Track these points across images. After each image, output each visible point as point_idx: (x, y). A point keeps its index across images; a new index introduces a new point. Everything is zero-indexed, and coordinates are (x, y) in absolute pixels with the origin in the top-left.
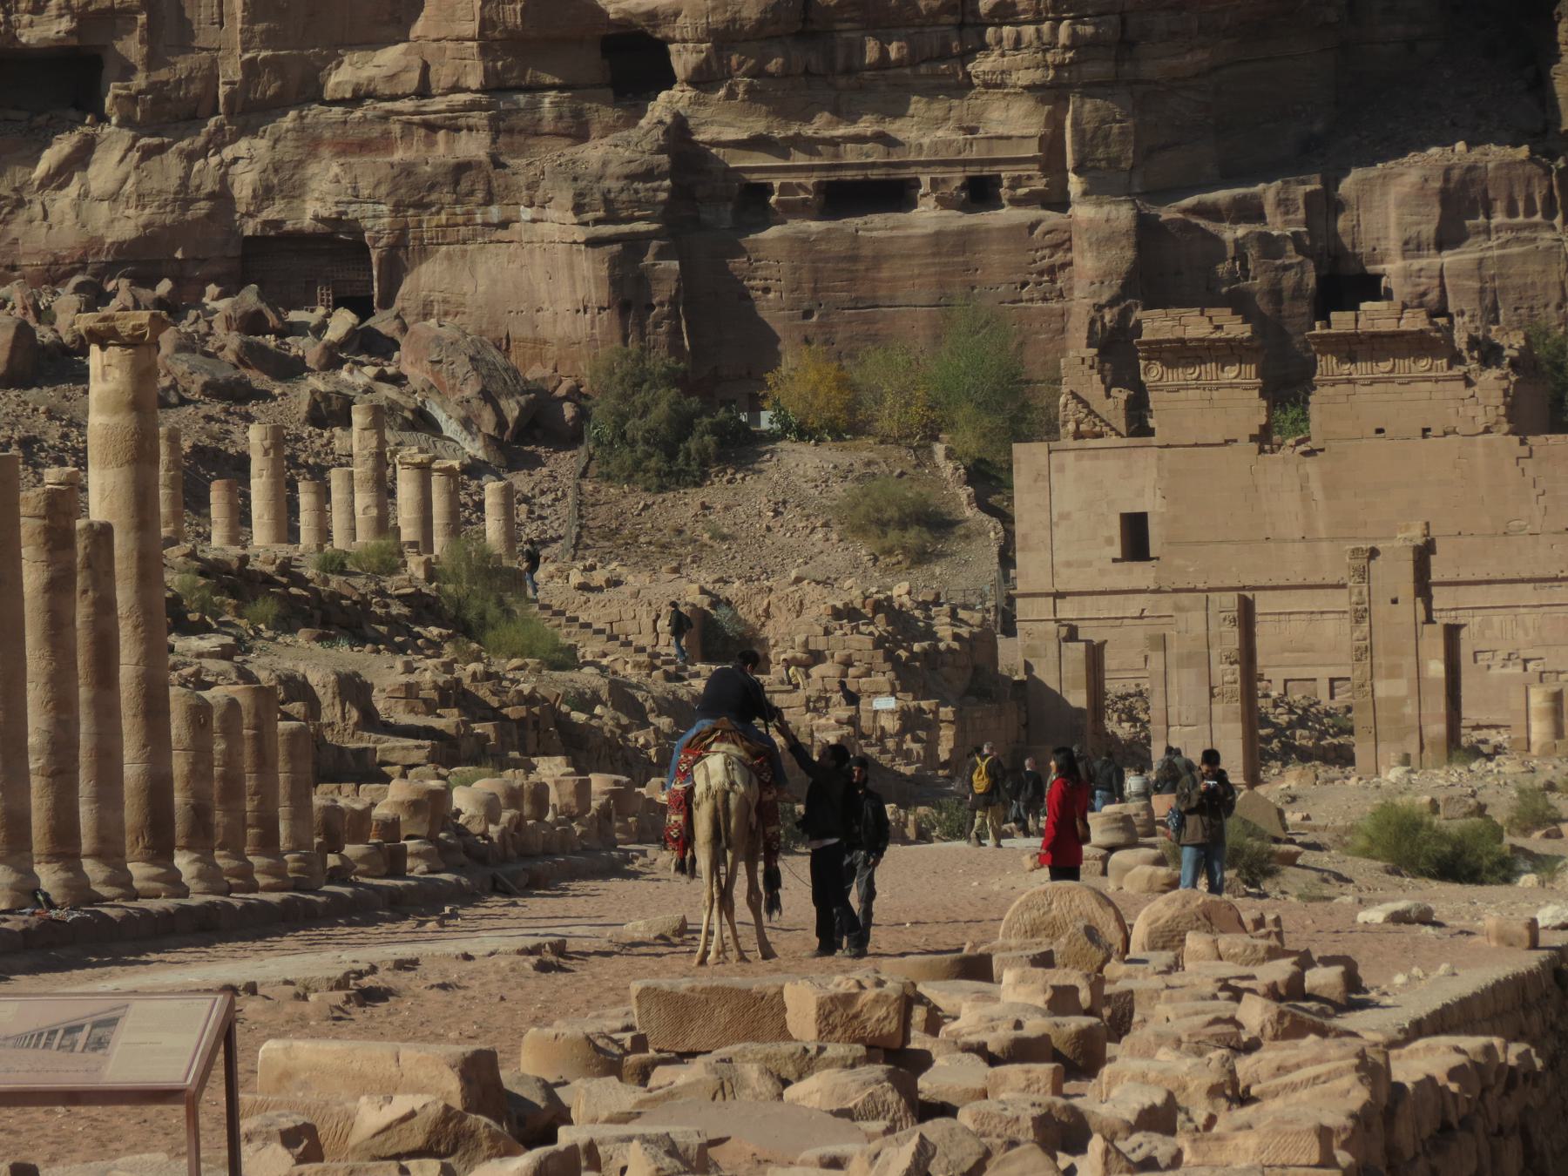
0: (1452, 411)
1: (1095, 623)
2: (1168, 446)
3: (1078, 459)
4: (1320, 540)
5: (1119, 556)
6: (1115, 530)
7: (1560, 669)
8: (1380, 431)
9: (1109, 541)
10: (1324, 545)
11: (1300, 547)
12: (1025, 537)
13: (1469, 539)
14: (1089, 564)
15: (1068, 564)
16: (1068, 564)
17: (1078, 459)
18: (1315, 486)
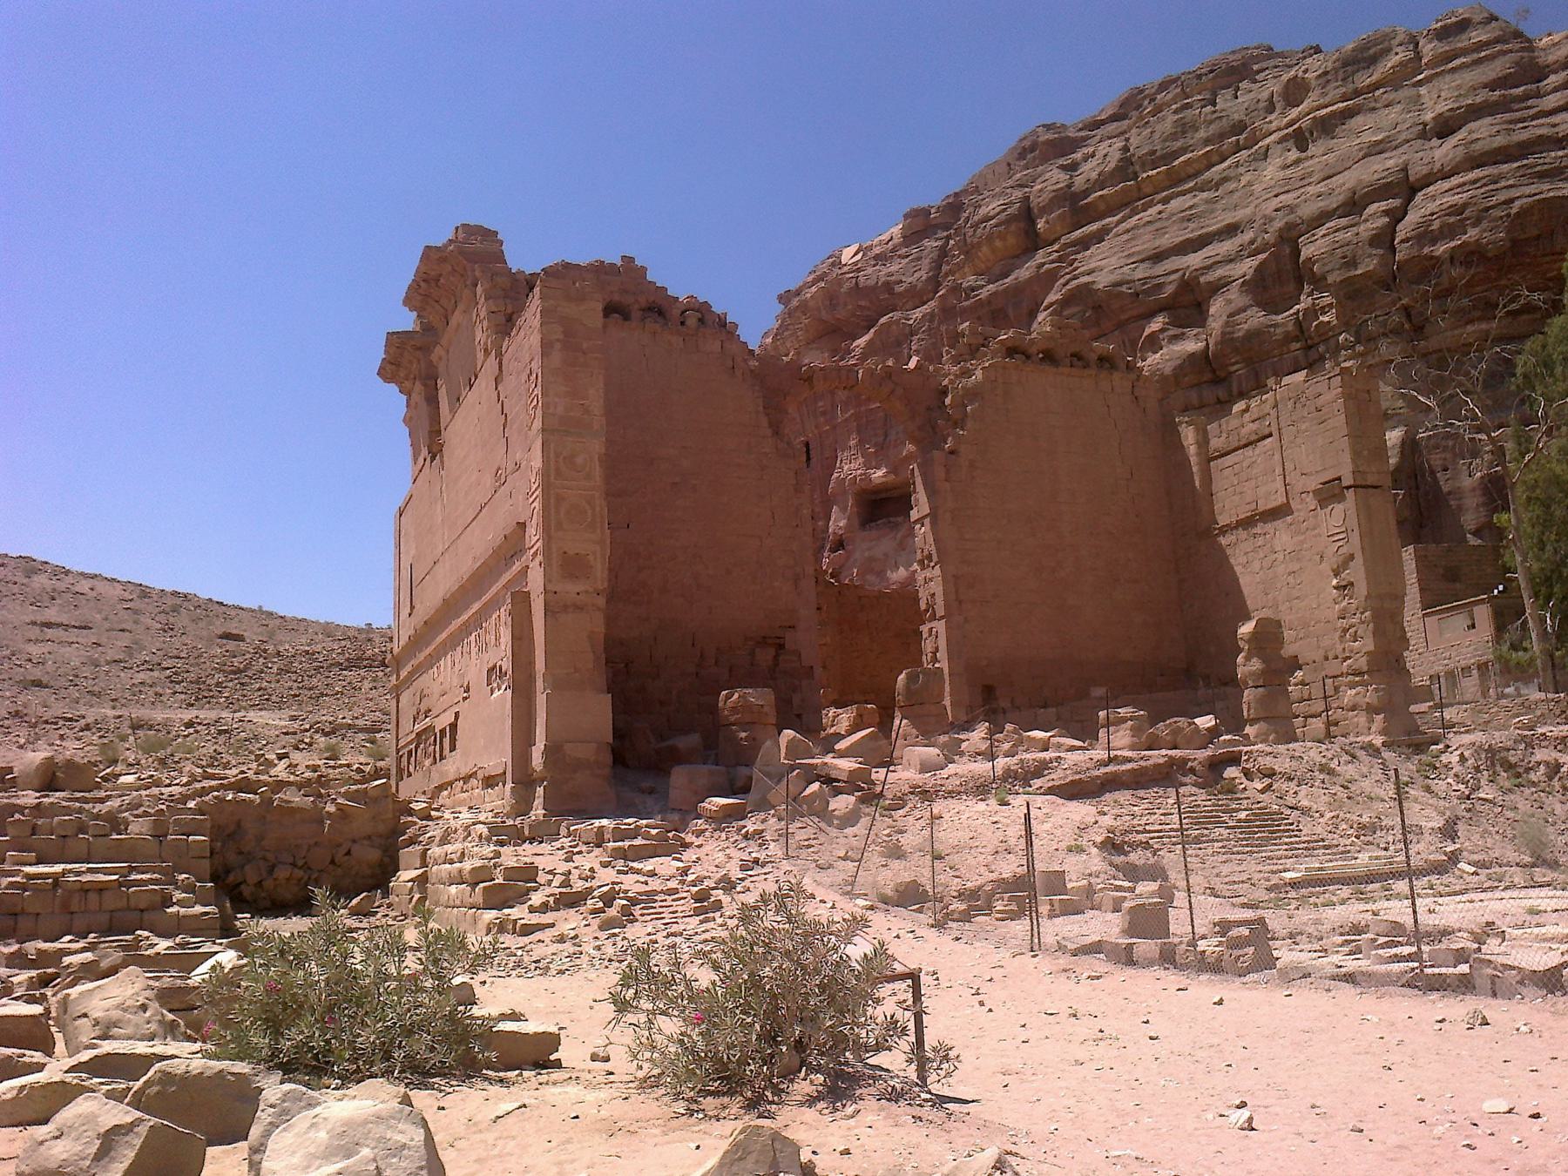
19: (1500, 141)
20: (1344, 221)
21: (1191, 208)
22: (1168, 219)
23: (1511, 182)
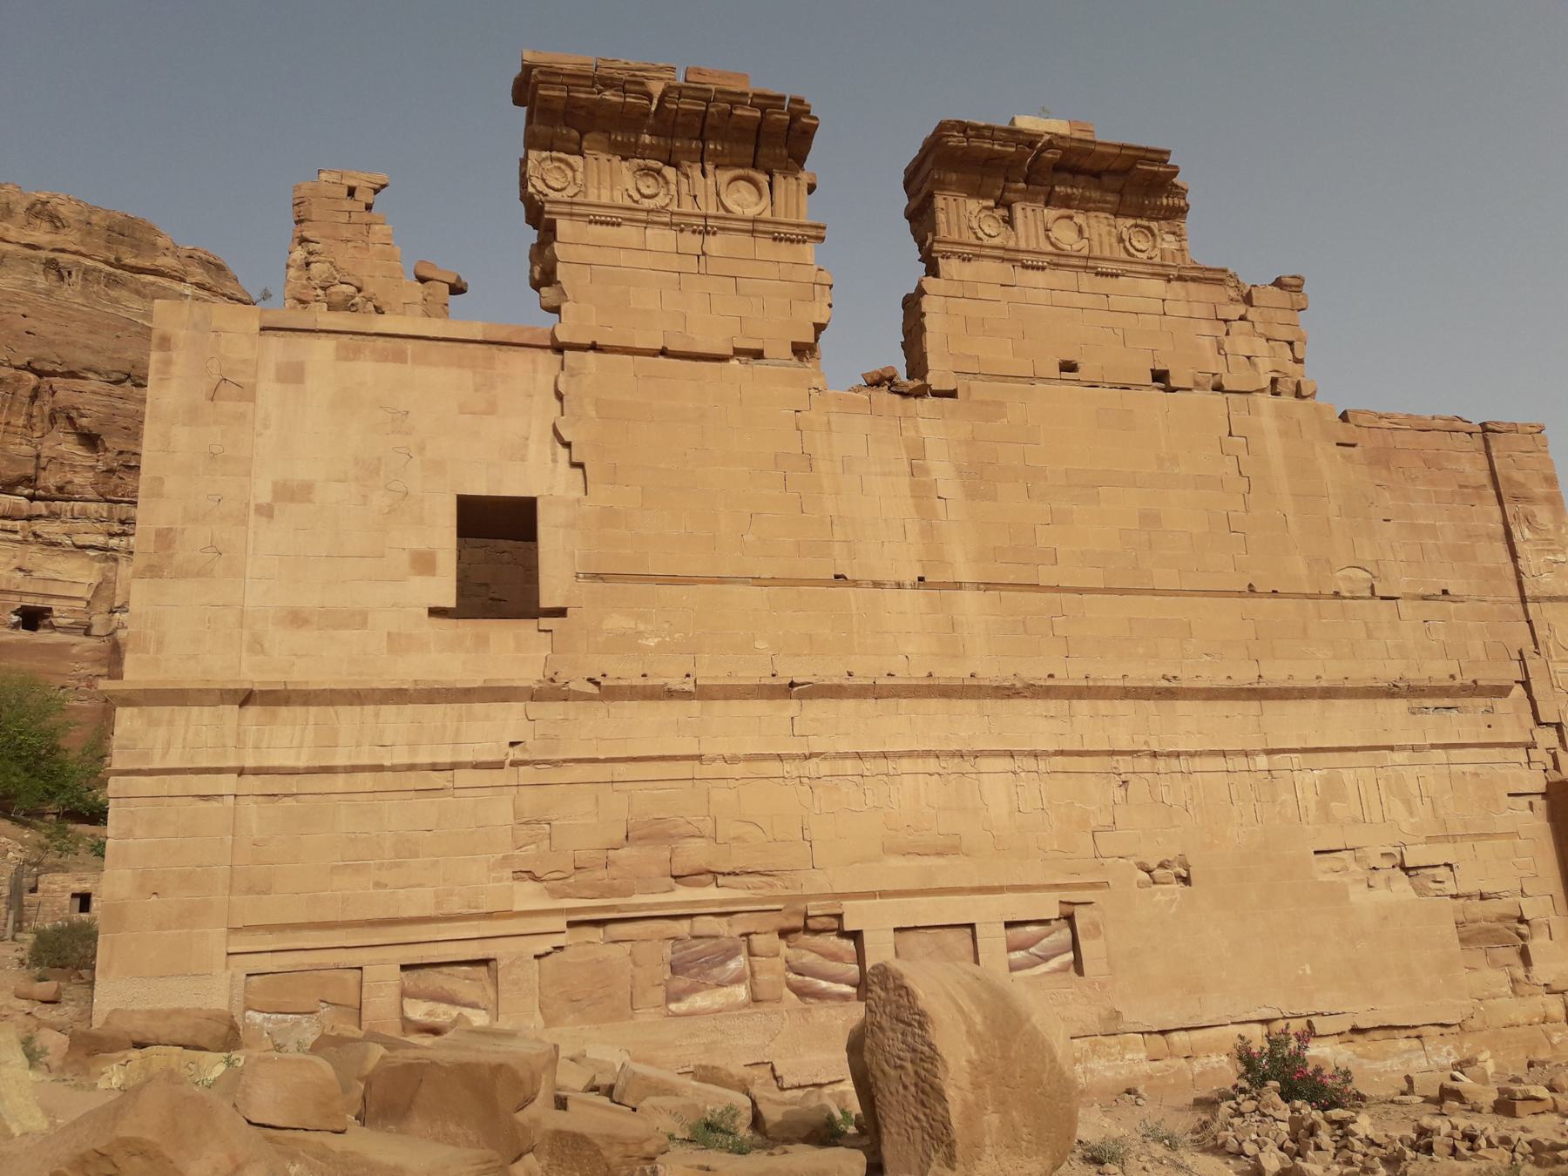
1: (365, 780)
4: (958, 586)
5: (450, 601)
8: (1068, 367)
9: (424, 563)
11: (913, 600)
14: (360, 619)
18: (941, 470)
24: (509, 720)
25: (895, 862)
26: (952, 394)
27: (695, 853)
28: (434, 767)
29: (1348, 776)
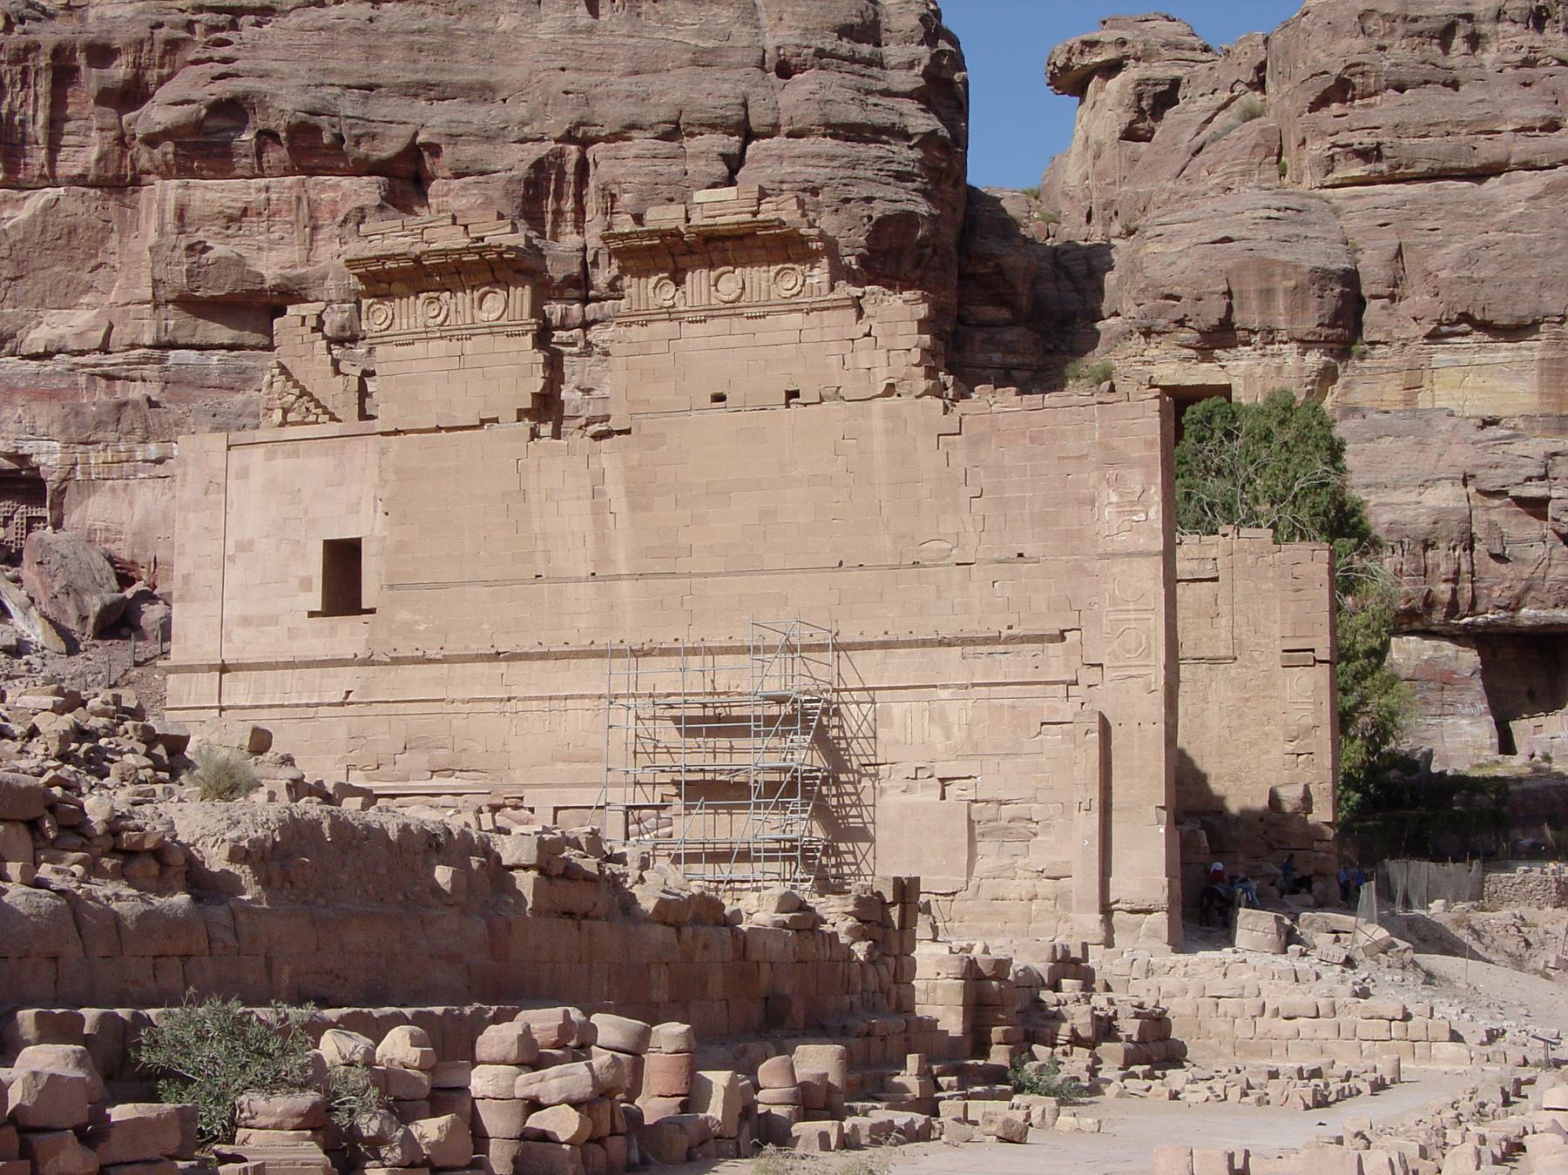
0: (835, 361)
2: (397, 432)
3: (270, 457)
4: (618, 577)
6: (314, 566)
7: (1004, 797)
8: (719, 398)
9: (306, 585)
10: (625, 586)
11: (588, 589)
12: (186, 578)
13: (856, 573)
14: (273, 620)
15: (246, 621)
16: (246, 621)
17: (270, 457)
18: (615, 491)
19: (855, 115)
20: (665, 147)
21: (421, 31)
22: (390, 34)
23: (869, 174)
24: (346, 678)
25: (560, 766)
26: (628, 432)
27: (442, 757)
28: (308, 705)
29: (897, 710)
